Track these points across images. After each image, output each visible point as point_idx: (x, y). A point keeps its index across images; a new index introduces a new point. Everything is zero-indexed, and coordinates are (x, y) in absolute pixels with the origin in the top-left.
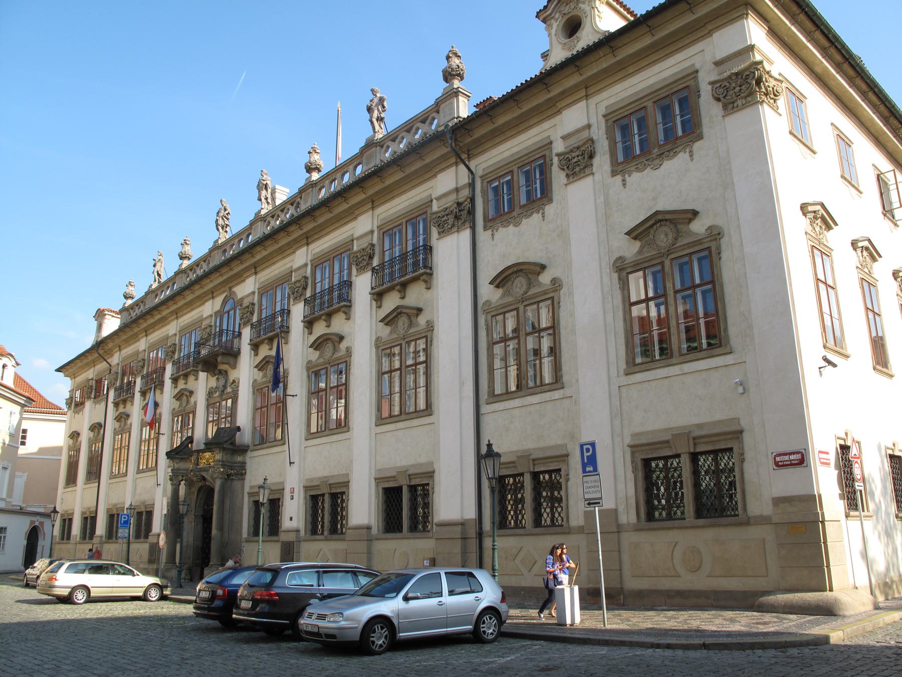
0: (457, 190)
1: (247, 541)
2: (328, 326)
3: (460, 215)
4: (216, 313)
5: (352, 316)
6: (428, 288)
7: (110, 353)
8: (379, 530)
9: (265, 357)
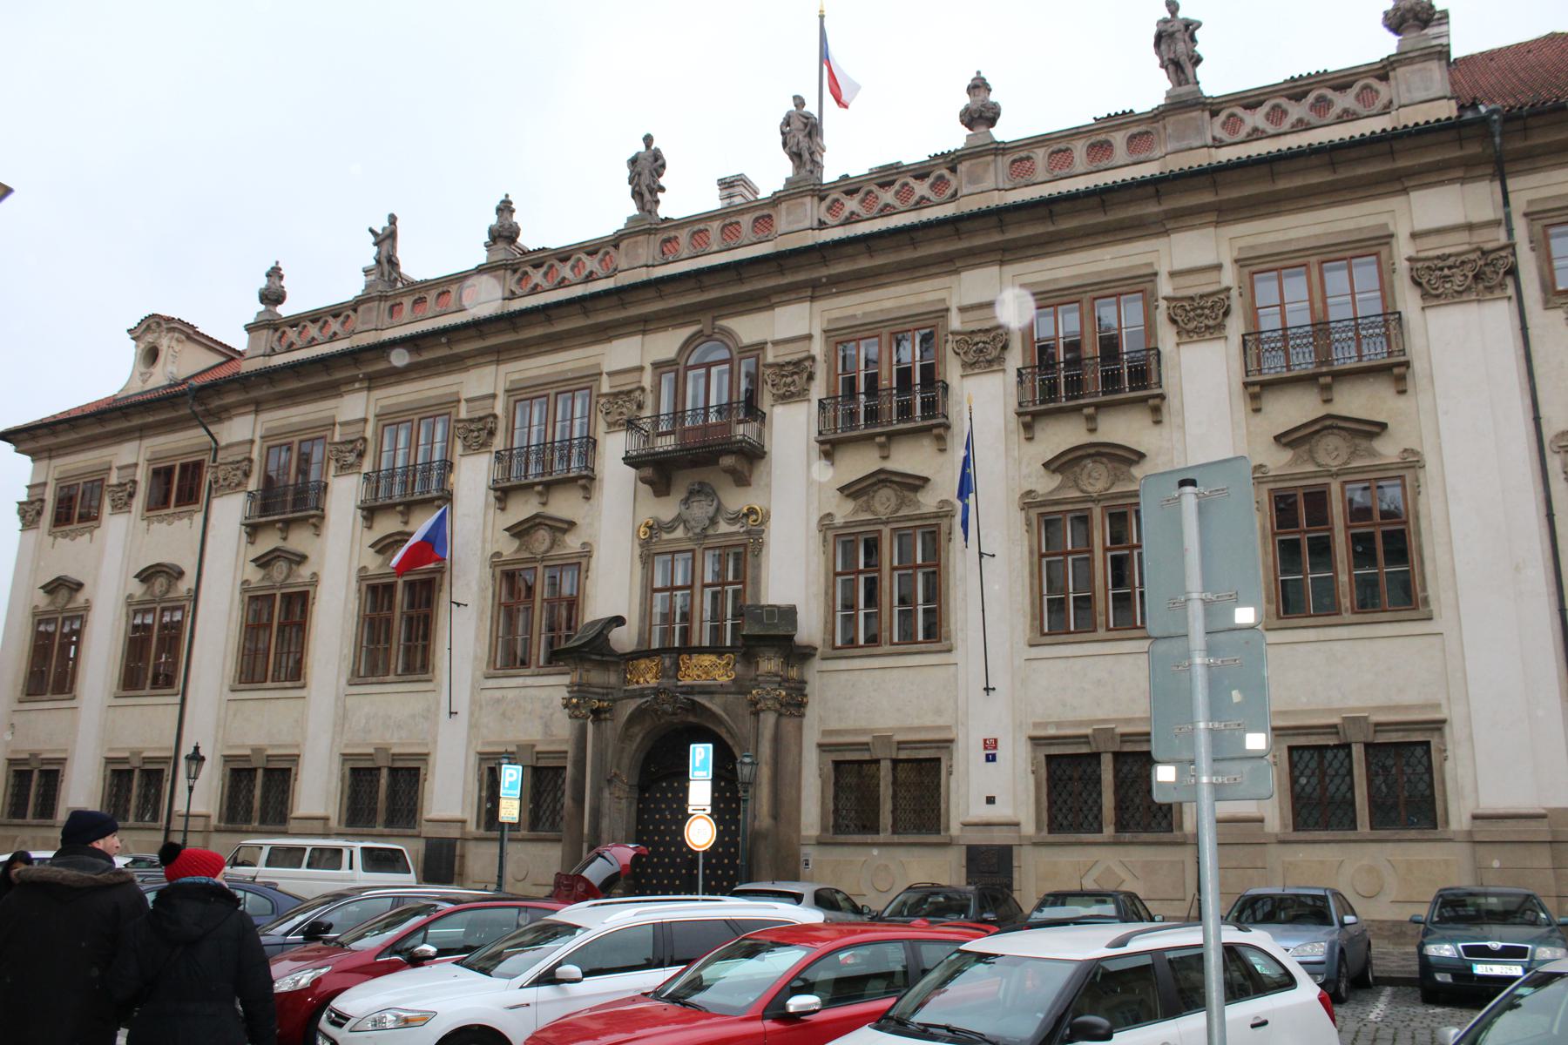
0: (1470, 227)
1: (820, 843)
2: (1092, 430)
3: (1478, 273)
4: (657, 366)
5: (1166, 418)
6: (1402, 392)
7: (222, 414)
8: (1284, 826)
9: (881, 471)
